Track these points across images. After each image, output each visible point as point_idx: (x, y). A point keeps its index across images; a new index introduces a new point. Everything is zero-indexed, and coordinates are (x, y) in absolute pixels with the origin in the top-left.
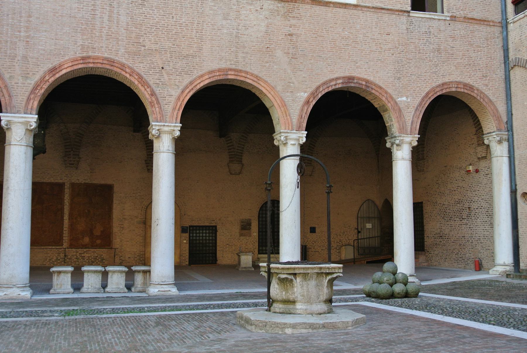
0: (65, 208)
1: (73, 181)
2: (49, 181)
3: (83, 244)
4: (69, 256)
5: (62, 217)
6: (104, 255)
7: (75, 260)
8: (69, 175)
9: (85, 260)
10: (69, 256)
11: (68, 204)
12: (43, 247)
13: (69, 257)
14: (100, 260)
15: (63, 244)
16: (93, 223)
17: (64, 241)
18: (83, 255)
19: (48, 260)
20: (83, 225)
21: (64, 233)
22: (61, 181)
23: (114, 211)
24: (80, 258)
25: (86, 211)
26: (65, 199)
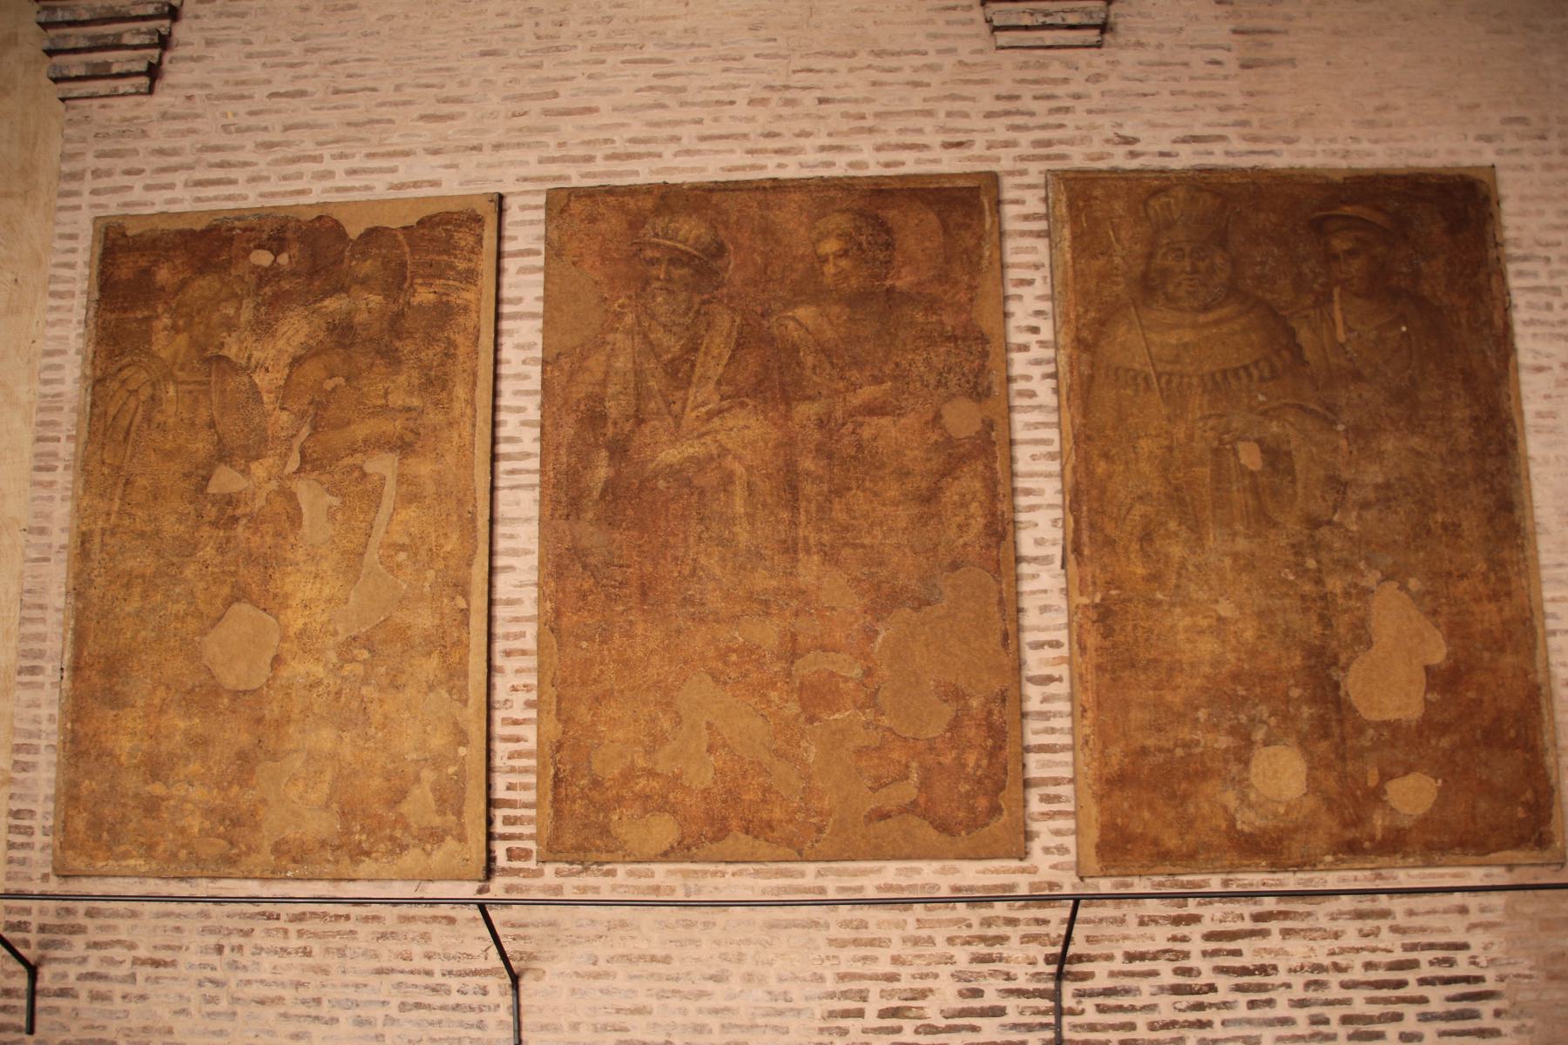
0: (1020, 434)
1: (1078, 159)
2: (840, 167)
3: (1248, 821)
4: (1100, 969)
5: (1001, 530)
6: (1477, 940)
7: (1167, 1008)
8: (1027, 103)
9: (1282, 1010)
10: (1100, 969)
11: (1045, 393)
12: (809, 876)
13: (1101, 981)
14: (1437, 998)
15: (1029, 836)
16: (1335, 584)
17: (1035, 806)
18: (1250, 953)
19: (872, 1020)
20: (1225, 609)
21: (1033, 704)
22: (950, 164)
23: (1534, 445)
24: (1224, 983)
25: (1250, 457)
26: (1016, 338)
